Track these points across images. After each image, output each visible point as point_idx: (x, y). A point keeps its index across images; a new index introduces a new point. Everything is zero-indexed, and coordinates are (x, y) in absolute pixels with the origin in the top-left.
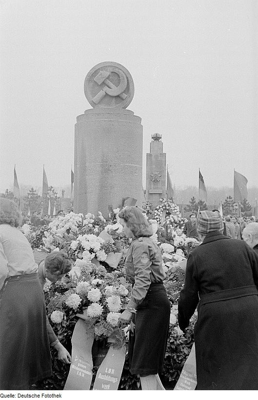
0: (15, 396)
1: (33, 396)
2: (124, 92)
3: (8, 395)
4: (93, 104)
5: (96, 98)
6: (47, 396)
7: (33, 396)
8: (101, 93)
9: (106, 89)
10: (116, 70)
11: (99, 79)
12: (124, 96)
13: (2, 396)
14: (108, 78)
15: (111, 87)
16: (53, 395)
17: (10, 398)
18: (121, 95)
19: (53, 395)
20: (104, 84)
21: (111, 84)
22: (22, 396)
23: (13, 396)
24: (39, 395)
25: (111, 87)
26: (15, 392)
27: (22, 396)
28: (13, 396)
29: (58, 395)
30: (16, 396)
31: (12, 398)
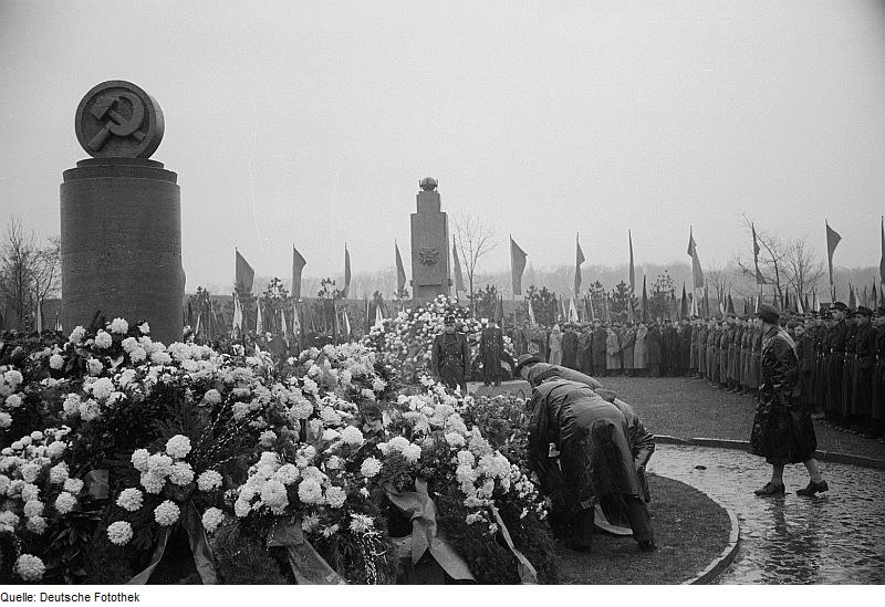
1: (75, 598)
2: (140, 129)
3: (19, 596)
4: (89, 150)
6: (108, 598)
7: (75, 598)
8: (103, 132)
9: (110, 124)
10: (127, 95)
11: (99, 110)
12: (140, 135)
13: (4, 597)
14: (114, 106)
16: (120, 597)
18: (135, 134)
19: (120, 597)
20: (106, 118)
21: (119, 117)
22: (51, 598)
23: (29, 598)
24: (88, 597)
25: (118, 126)
27: (51, 598)
28: (29, 598)
29: (131, 597)
30: (37, 598)
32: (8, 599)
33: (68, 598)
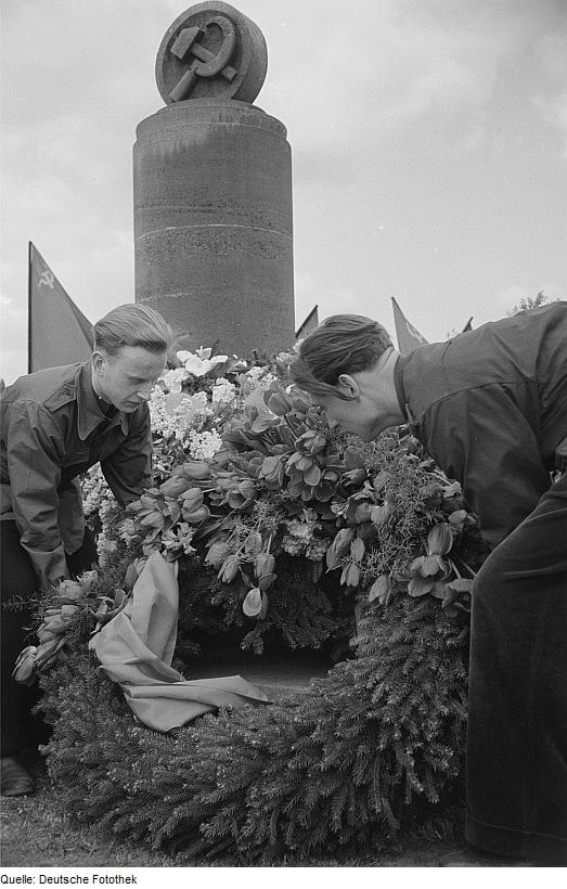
0: (34, 880)
1: (73, 880)
3: (19, 879)
4: (170, 101)
5: (176, 92)
6: (106, 880)
7: (73, 880)
8: (187, 76)
9: (196, 63)
11: (179, 50)
13: (4, 879)
14: (199, 38)
16: (118, 879)
17: (22, 886)
19: (118, 879)
20: (190, 57)
22: (50, 880)
23: (28, 880)
24: (86, 879)
26: (33, 872)
27: (50, 880)
28: (28, 880)
29: (128, 879)
30: (37, 880)
31: (27, 886)
33: (67, 881)
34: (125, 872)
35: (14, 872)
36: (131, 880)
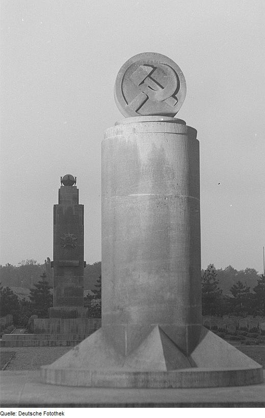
0: (16, 414)
1: (34, 414)
3: (9, 413)
6: (50, 414)
7: (34, 414)
13: (2, 413)
15: (69, 182)
16: (55, 413)
19: (55, 413)
22: (23, 414)
23: (13, 414)
24: (40, 413)
25: (69, 182)
27: (23, 414)
28: (13, 414)
29: (60, 413)
30: (17, 414)
32: (4, 414)
33: (31, 414)
34: (59, 410)
35: (6, 410)
36: (62, 414)
